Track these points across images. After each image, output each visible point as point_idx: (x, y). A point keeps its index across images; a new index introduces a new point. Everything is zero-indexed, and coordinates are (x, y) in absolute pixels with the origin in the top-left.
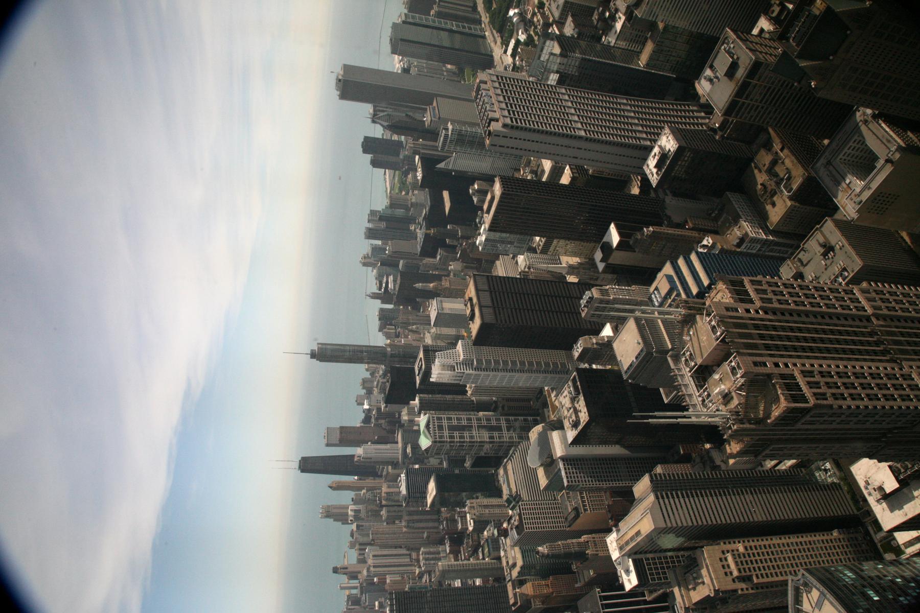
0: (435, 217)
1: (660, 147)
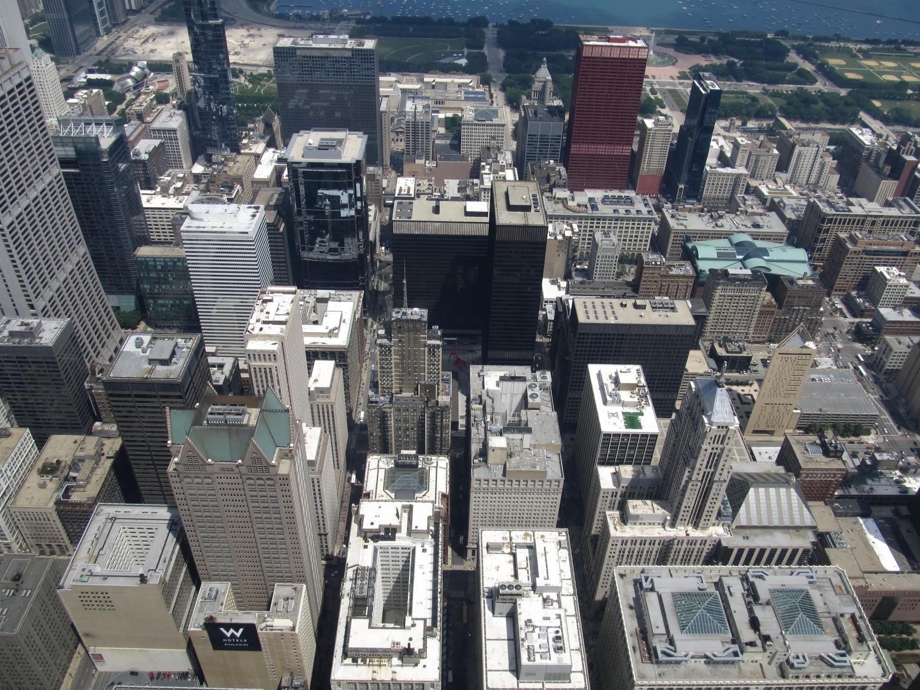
1: (40, 324)
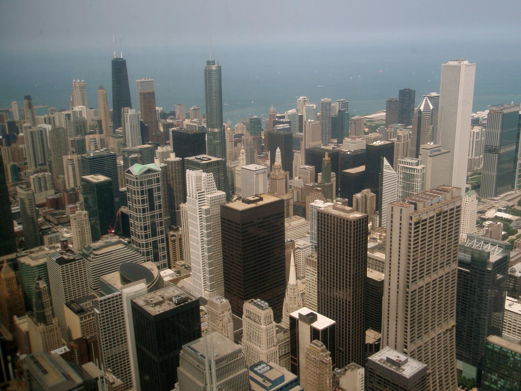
0: (339, 161)
1: (406, 361)
